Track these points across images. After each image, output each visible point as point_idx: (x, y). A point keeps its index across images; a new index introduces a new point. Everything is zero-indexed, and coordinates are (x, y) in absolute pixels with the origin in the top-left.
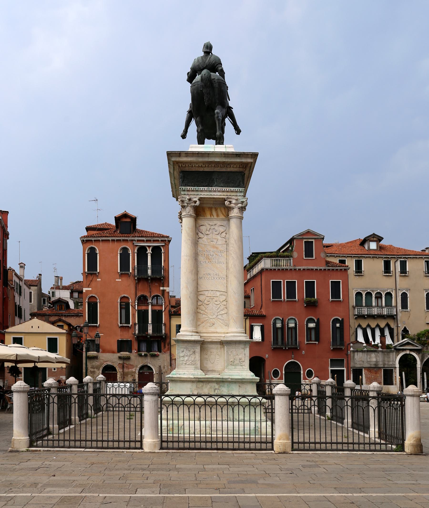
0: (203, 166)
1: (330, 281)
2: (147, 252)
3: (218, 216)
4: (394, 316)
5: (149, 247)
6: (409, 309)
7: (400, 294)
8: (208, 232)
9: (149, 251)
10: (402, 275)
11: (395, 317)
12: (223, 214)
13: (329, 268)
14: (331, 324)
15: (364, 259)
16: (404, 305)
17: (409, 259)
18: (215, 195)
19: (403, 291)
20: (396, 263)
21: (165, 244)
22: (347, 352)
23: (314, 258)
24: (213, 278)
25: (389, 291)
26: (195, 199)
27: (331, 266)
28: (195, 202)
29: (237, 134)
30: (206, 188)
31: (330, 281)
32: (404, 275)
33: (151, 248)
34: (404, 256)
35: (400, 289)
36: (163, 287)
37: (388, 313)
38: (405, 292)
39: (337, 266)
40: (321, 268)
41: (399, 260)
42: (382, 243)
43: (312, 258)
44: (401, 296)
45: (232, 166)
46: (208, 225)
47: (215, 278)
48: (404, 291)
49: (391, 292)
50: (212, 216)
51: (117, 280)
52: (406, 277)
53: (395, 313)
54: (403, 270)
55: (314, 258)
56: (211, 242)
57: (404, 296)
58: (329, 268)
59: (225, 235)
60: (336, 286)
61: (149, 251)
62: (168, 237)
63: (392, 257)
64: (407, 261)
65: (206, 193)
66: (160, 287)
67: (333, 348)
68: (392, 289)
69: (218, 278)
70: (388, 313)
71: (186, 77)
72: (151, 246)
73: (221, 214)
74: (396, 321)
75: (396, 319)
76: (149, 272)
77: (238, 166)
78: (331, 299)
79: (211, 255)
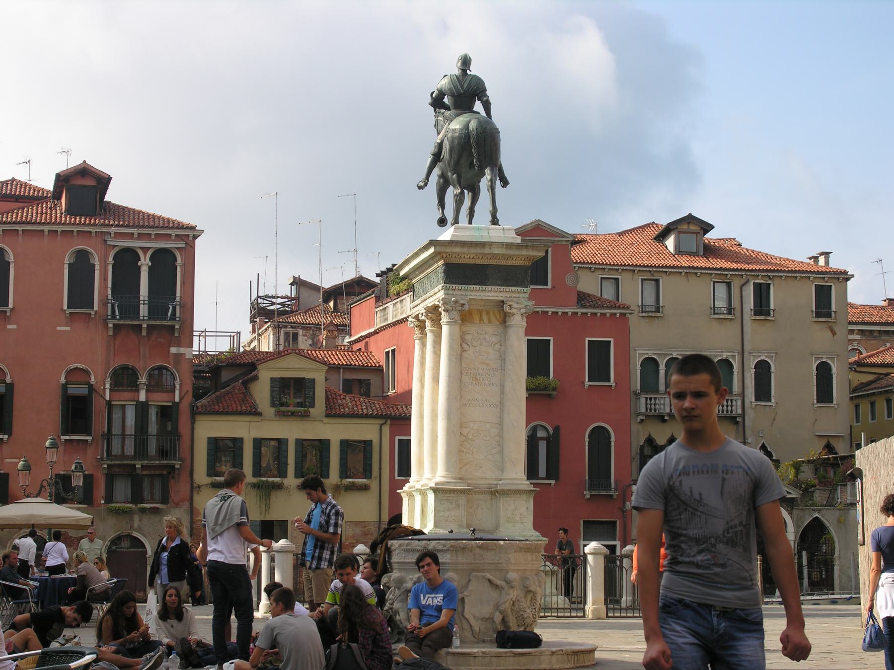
0: (475, 257)
1: (587, 339)
2: (139, 264)
3: (490, 321)
4: (736, 417)
5: (145, 250)
6: (773, 400)
7: (751, 364)
8: (475, 343)
9: (145, 263)
10: (757, 318)
11: (738, 420)
12: (497, 320)
13: (585, 311)
14: (587, 439)
15: (664, 276)
16: (763, 392)
17: (776, 281)
18: (488, 296)
19: (760, 356)
20: (744, 288)
21: (186, 243)
22: (624, 504)
23: (549, 286)
24: (481, 406)
25: (724, 357)
26: (462, 302)
27: (590, 307)
28: (463, 305)
29: (503, 187)
30: (478, 287)
31: (587, 339)
32: (762, 318)
33: (149, 254)
34: (764, 274)
35: (753, 353)
36: (179, 346)
37: (723, 411)
38: (767, 359)
39: (603, 306)
40: (566, 310)
41: (753, 282)
42: (711, 235)
43: (545, 287)
44: (755, 368)
45: (514, 259)
46: (475, 335)
47: (485, 406)
48: (763, 358)
49: (731, 360)
50: (482, 322)
51: (59, 328)
52: (768, 325)
53: (740, 411)
54: (762, 307)
55: (549, 286)
56: (480, 357)
57: (763, 369)
58: (585, 311)
59: (499, 347)
60: (599, 352)
61: (145, 263)
62: (193, 228)
63: (735, 275)
64: (771, 286)
65: (478, 294)
66: (169, 346)
67: (591, 495)
68: (734, 352)
69: (489, 406)
70: (723, 411)
71: (429, 100)
72: (148, 248)
73: (494, 319)
74: (741, 429)
75: (741, 424)
76: (144, 310)
77: (523, 259)
78: (589, 381)
79: (479, 374)
